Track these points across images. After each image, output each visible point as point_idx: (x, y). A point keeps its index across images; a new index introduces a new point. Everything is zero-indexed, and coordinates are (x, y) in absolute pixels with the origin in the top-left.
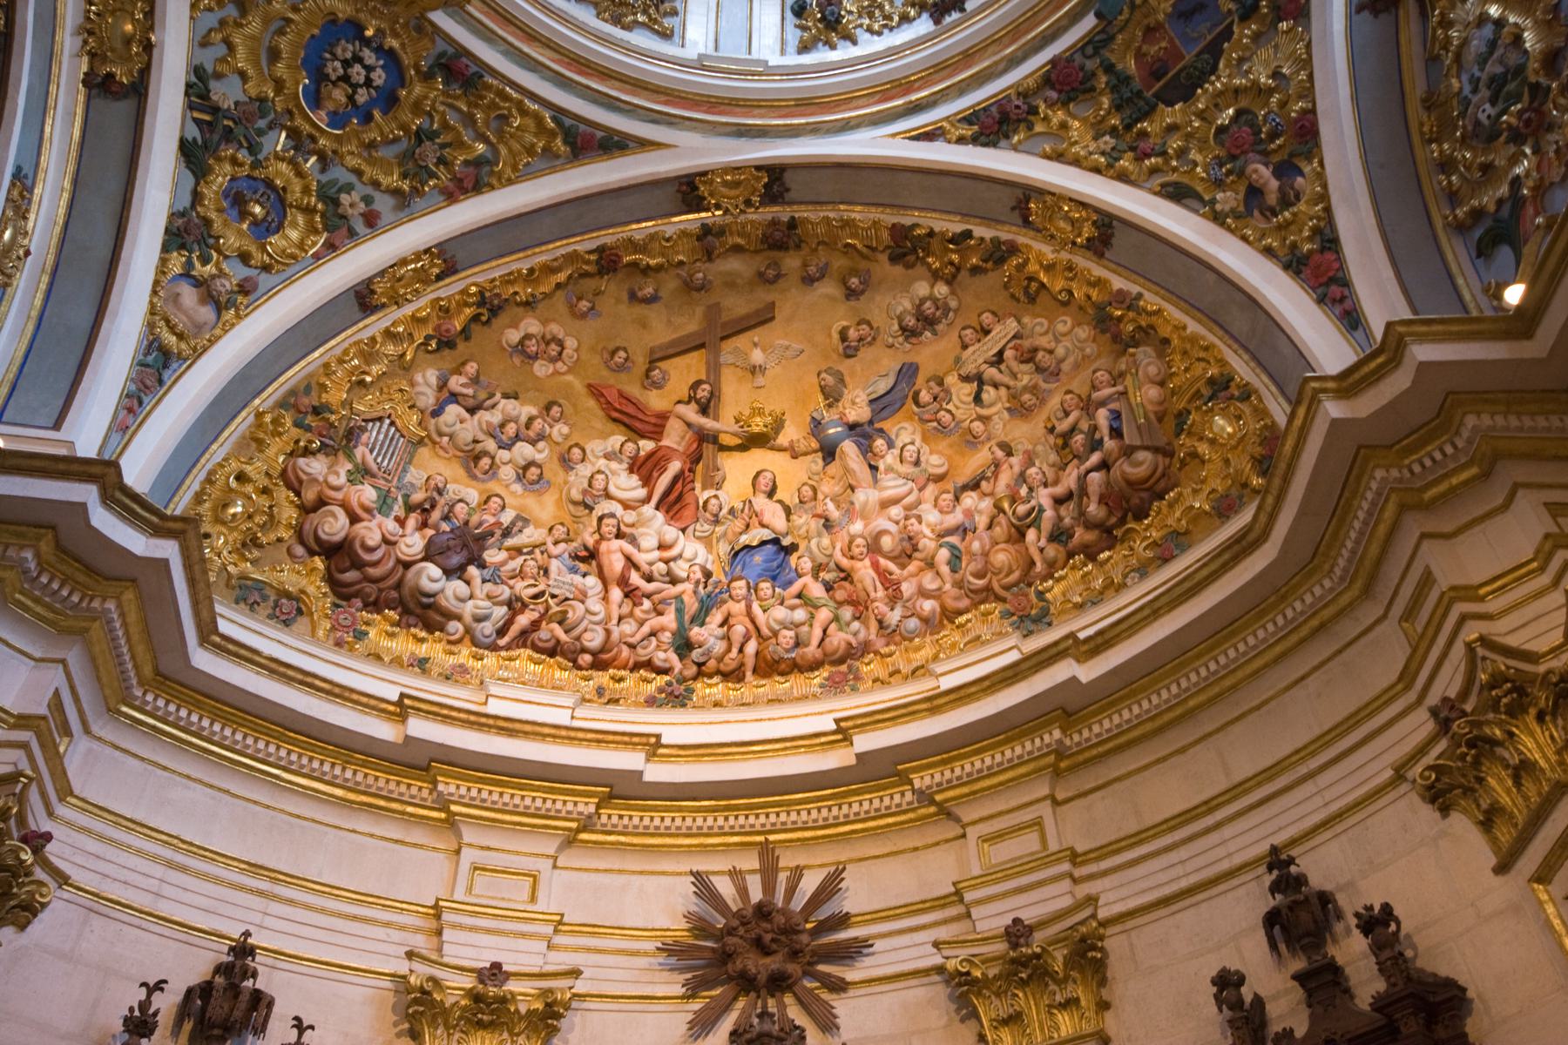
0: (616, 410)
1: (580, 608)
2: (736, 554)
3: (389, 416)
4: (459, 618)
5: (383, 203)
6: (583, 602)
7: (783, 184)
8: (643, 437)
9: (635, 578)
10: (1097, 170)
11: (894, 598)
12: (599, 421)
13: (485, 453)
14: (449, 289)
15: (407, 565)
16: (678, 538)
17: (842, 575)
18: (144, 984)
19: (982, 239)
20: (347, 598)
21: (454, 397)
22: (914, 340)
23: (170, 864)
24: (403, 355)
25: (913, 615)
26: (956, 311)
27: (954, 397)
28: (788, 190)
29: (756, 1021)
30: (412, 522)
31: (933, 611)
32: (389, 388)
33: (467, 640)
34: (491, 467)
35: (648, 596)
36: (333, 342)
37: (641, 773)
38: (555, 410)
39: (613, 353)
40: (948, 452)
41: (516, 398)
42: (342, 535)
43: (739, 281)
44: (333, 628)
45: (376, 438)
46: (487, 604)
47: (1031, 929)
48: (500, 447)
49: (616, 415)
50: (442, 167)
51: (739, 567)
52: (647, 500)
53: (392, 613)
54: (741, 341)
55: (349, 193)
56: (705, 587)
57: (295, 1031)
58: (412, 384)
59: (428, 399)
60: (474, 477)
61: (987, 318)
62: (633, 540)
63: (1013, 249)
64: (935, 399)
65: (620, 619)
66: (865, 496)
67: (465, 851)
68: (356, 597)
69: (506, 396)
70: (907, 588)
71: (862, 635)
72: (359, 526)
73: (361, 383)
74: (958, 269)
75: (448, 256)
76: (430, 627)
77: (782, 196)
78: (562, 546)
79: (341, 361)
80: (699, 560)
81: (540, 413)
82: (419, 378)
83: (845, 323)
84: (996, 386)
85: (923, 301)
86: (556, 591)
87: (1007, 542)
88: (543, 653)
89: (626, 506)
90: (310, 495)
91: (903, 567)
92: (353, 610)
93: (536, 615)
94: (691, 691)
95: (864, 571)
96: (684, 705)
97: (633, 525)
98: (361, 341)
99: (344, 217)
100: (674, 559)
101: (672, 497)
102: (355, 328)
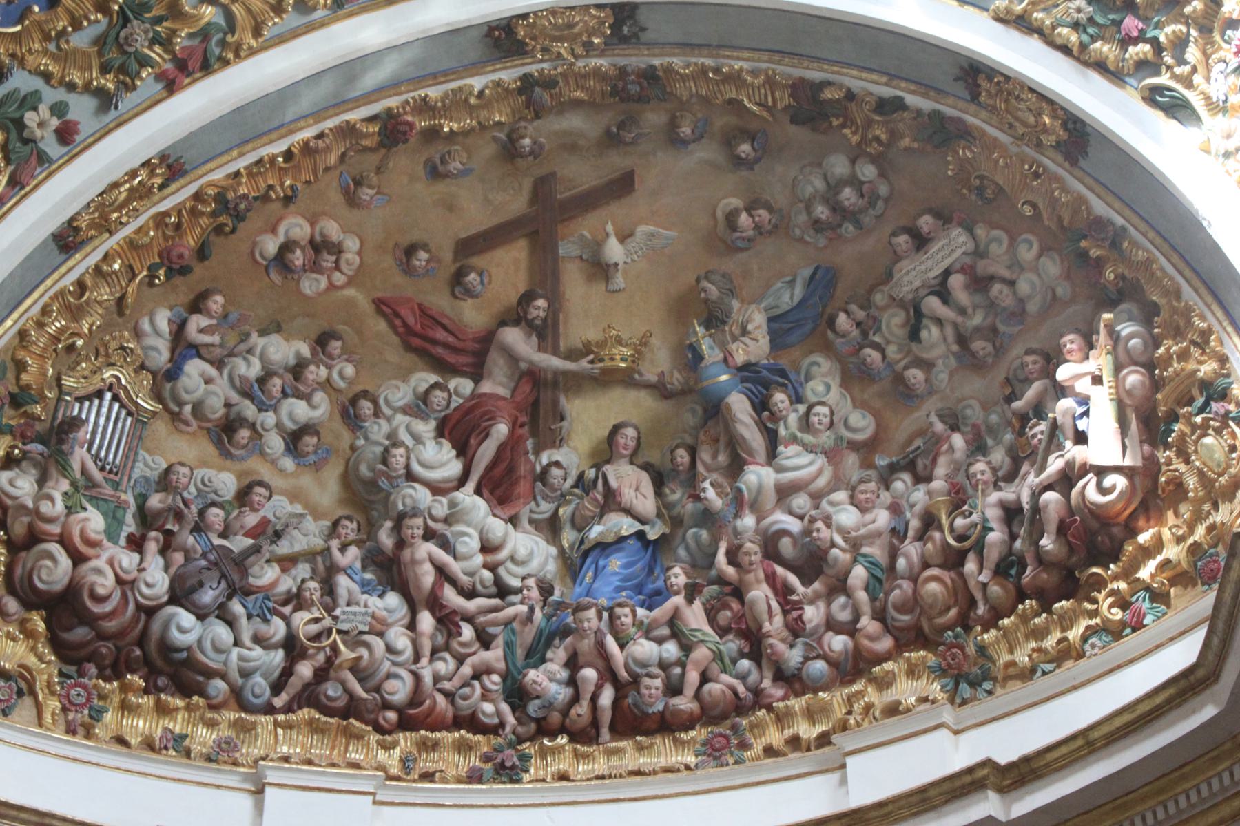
0: (416, 335)
1: (378, 644)
2: (586, 554)
3: (110, 388)
4: (223, 676)
5: (81, 108)
6: (381, 634)
7: (635, 23)
8: (455, 371)
9: (450, 596)
10: (1065, 49)
11: (796, 630)
12: (394, 353)
13: (241, 421)
14: (181, 194)
15: (151, 612)
16: (506, 534)
17: (727, 589)
19: (919, 112)
20: (78, 663)
21: (196, 350)
22: (829, 233)
24: (121, 301)
25: (817, 657)
26: (886, 200)
27: (884, 327)
28: (643, 29)
30: (152, 547)
31: (845, 645)
32: (106, 346)
33: (232, 703)
34: (251, 439)
35: (469, 619)
36: (29, 301)
38: (335, 346)
39: (411, 251)
40: (877, 404)
41: (278, 329)
42: (66, 581)
43: (581, 142)
44: (64, 709)
45: (96, 424)
46: (258, 651)
48: (260, 410)
49: (416, 342)
50: (157, 49)
51: (590, 573)
52: (462, 481)
53: (136, 678)
54: (585, 227)
55: (35, 109)
56: (542, 608)
58: (138, 334)
59: (161, 356)
60: (226, 454)
61: (926, 223)
62: (446, 545)
63: (965, 133)
64: (858, 324)
65: (434, 652)
66: (758, 476)
68: (89, 661)
69: (263, 333)
70: (813, 614)
71: (754, 677)
72: (85, 567)
73: (71, 348)
74: (889, 145)
75: (170, 161)
76: (185, 690)
77: (636, 36)
78: (353, 551)
79: (40, 325)
80: (534, 565)
81: (314, 353)
82: (146, 325)
83: (735, 202)
84: (939, 322)
85: (842, 183)
86: (345, 627)
87: (939, 566)
88: (331, 716)
89: (437, 490)
90: (19, 527)
91: (806, 582)
92: (85, 681)
93: (321, 658)
94: (525, 758)
95: (760, 593)
96: (518, 781)
97: (447, 521)
98: (62, 293)
99: (26, 141)
100: (501, 563)
101: (498, 471)
102: (56, 276)
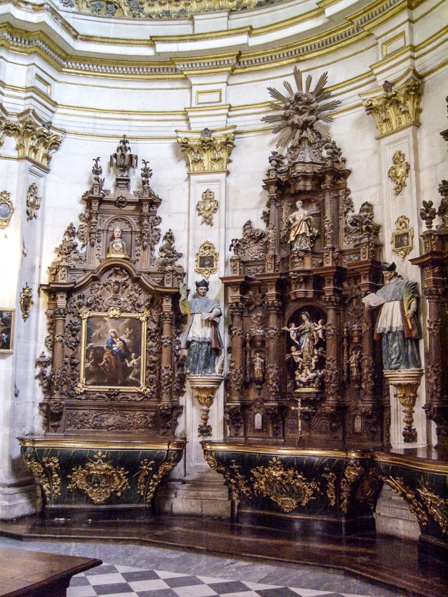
18: (94, 159)
23: (95, 117)
37: (247, 44)
44: (131, 10)
47: (393, 84)
57: (144, 164)
67: (193, 87)
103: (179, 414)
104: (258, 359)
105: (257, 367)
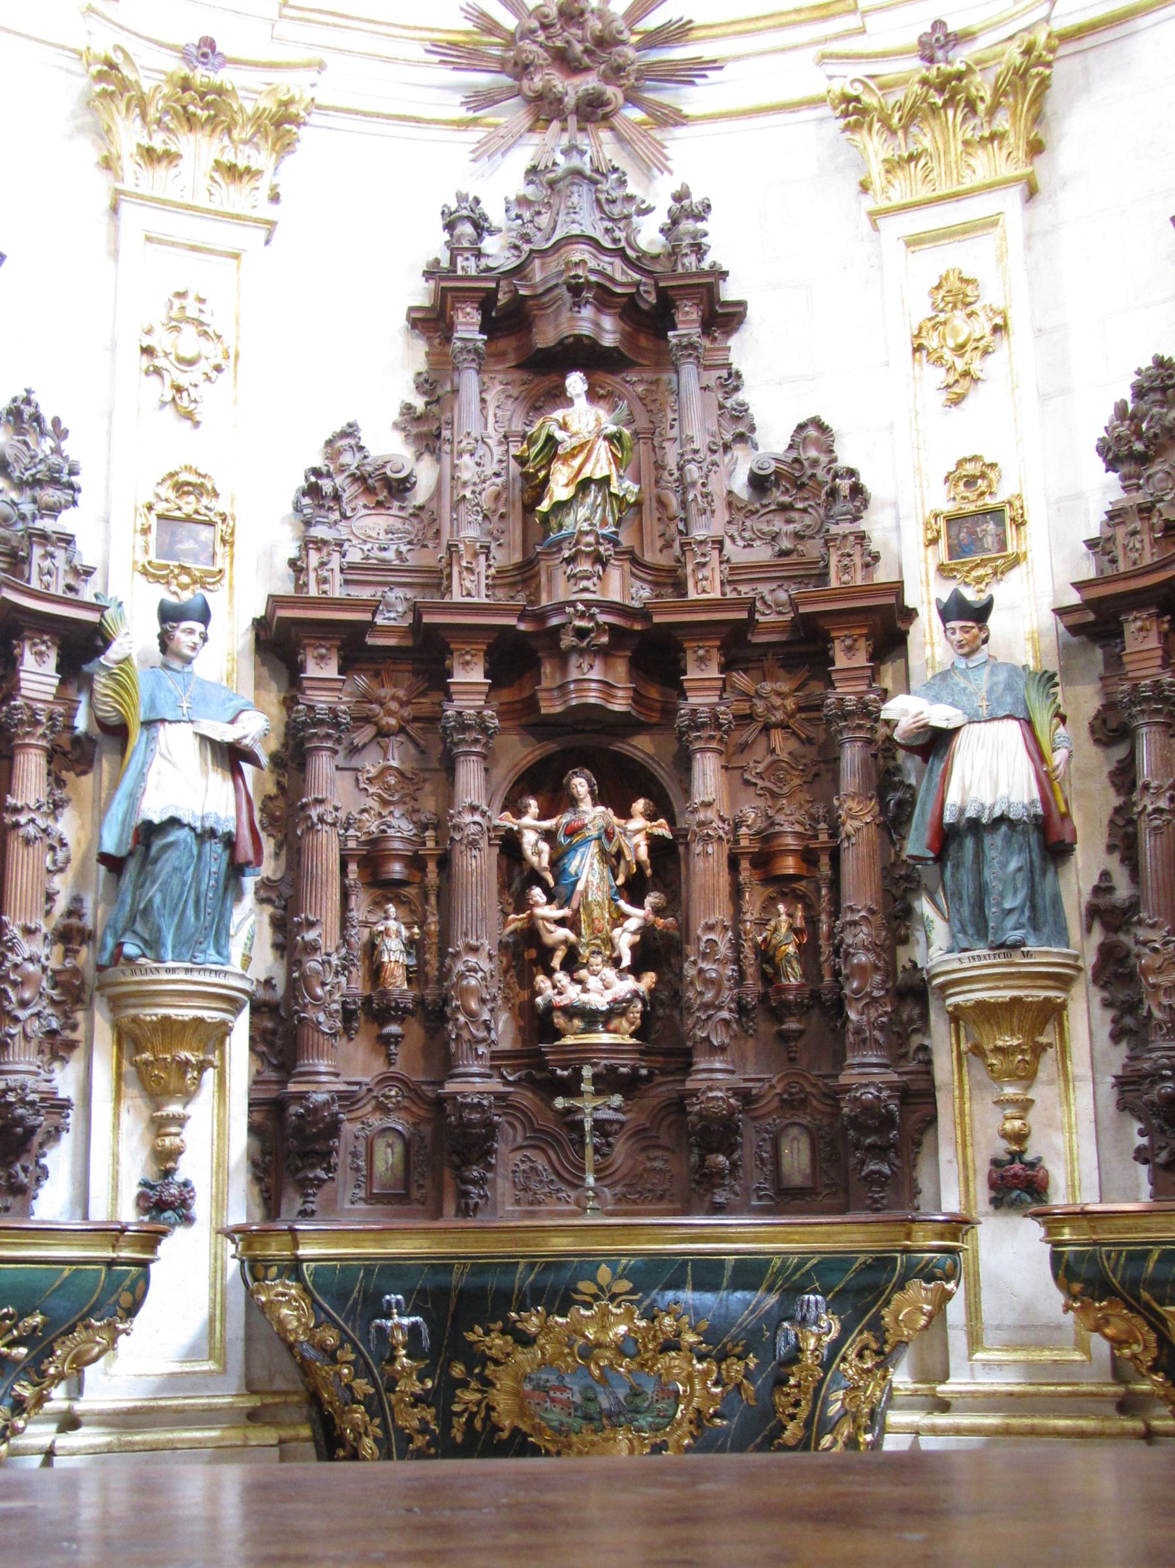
29: (560, 159)
103: (55, 1134)
104: (392, 925)
105: (394, 953)
